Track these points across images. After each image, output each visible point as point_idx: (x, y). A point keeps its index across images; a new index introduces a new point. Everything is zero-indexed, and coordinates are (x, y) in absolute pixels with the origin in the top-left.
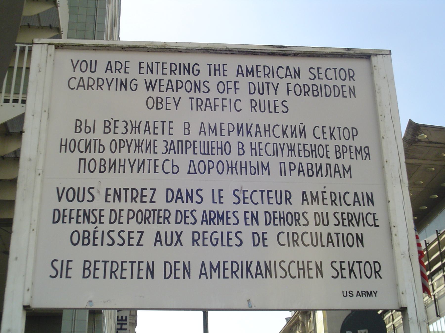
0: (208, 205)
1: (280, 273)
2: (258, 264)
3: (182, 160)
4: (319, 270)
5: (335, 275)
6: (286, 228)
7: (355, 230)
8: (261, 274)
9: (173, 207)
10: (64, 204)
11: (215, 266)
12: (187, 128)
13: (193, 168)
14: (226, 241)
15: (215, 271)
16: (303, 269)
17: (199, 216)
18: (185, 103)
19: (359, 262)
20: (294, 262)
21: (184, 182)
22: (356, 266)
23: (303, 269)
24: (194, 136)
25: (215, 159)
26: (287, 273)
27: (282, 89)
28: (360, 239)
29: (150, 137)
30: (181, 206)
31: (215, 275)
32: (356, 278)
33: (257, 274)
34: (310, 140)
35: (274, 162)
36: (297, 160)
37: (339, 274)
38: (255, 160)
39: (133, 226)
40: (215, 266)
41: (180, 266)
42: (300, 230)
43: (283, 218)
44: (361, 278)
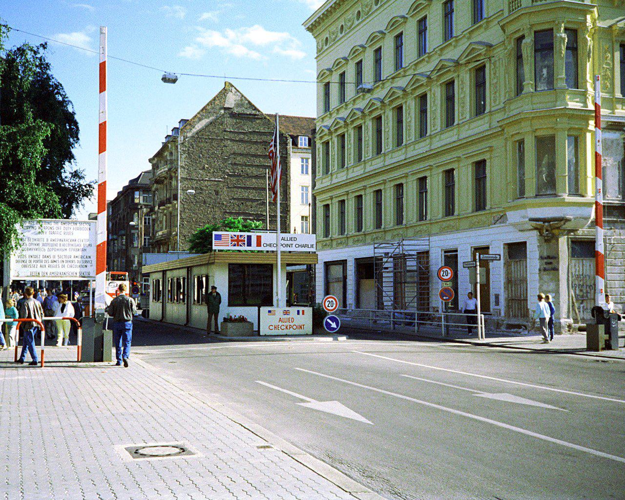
0: (52, 259)
3: (46, 248)
6: (70, 264)
7: (85, 264)
9: (43, 259)
10: (20, 259)
12: (47, 240)
13: (49, 250)
14: (56, 266)
17: (50, 261)
18: (48, 233)
21: (47, 253)
24: (49, 242)
25: (54, 248)
27: (72, 229)
28: (86, 266)
29: (38, 242)
30: (46, 259)
34: (77, 243)
35: (68, 248)
36: (73, 248)
38: (63, 248)
39: (35, 263)
42: (72, 264)
43: (70, 262)
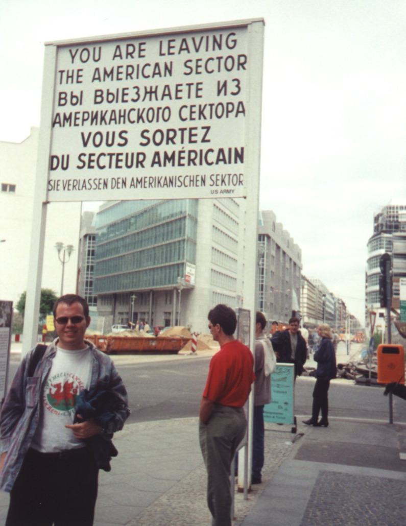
1: (178, 183)
2: (166, 179)
4: (203, 181)
5: (212, 183)
8: (167, 184)
11: (139, 180)
15: (139, 183)
16: (193, 181)
19: (229, 175)
20: (187, 176)
22: (227, 178)
23: (193, 181)
26: (183, 184)
31: (139, 186)
32: (225, 185)
33: (164, 184)
37: (215, 183)
40: (139, 180)
41: (120, 181)
44: (229, 185)
